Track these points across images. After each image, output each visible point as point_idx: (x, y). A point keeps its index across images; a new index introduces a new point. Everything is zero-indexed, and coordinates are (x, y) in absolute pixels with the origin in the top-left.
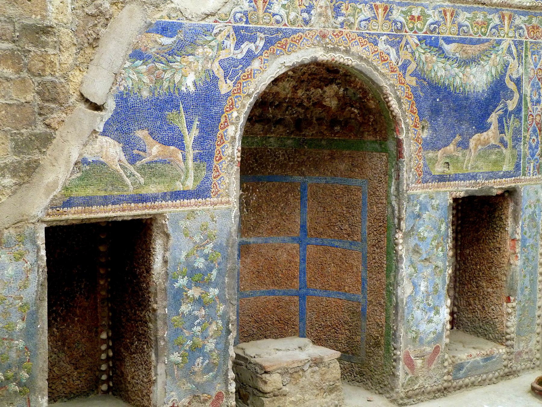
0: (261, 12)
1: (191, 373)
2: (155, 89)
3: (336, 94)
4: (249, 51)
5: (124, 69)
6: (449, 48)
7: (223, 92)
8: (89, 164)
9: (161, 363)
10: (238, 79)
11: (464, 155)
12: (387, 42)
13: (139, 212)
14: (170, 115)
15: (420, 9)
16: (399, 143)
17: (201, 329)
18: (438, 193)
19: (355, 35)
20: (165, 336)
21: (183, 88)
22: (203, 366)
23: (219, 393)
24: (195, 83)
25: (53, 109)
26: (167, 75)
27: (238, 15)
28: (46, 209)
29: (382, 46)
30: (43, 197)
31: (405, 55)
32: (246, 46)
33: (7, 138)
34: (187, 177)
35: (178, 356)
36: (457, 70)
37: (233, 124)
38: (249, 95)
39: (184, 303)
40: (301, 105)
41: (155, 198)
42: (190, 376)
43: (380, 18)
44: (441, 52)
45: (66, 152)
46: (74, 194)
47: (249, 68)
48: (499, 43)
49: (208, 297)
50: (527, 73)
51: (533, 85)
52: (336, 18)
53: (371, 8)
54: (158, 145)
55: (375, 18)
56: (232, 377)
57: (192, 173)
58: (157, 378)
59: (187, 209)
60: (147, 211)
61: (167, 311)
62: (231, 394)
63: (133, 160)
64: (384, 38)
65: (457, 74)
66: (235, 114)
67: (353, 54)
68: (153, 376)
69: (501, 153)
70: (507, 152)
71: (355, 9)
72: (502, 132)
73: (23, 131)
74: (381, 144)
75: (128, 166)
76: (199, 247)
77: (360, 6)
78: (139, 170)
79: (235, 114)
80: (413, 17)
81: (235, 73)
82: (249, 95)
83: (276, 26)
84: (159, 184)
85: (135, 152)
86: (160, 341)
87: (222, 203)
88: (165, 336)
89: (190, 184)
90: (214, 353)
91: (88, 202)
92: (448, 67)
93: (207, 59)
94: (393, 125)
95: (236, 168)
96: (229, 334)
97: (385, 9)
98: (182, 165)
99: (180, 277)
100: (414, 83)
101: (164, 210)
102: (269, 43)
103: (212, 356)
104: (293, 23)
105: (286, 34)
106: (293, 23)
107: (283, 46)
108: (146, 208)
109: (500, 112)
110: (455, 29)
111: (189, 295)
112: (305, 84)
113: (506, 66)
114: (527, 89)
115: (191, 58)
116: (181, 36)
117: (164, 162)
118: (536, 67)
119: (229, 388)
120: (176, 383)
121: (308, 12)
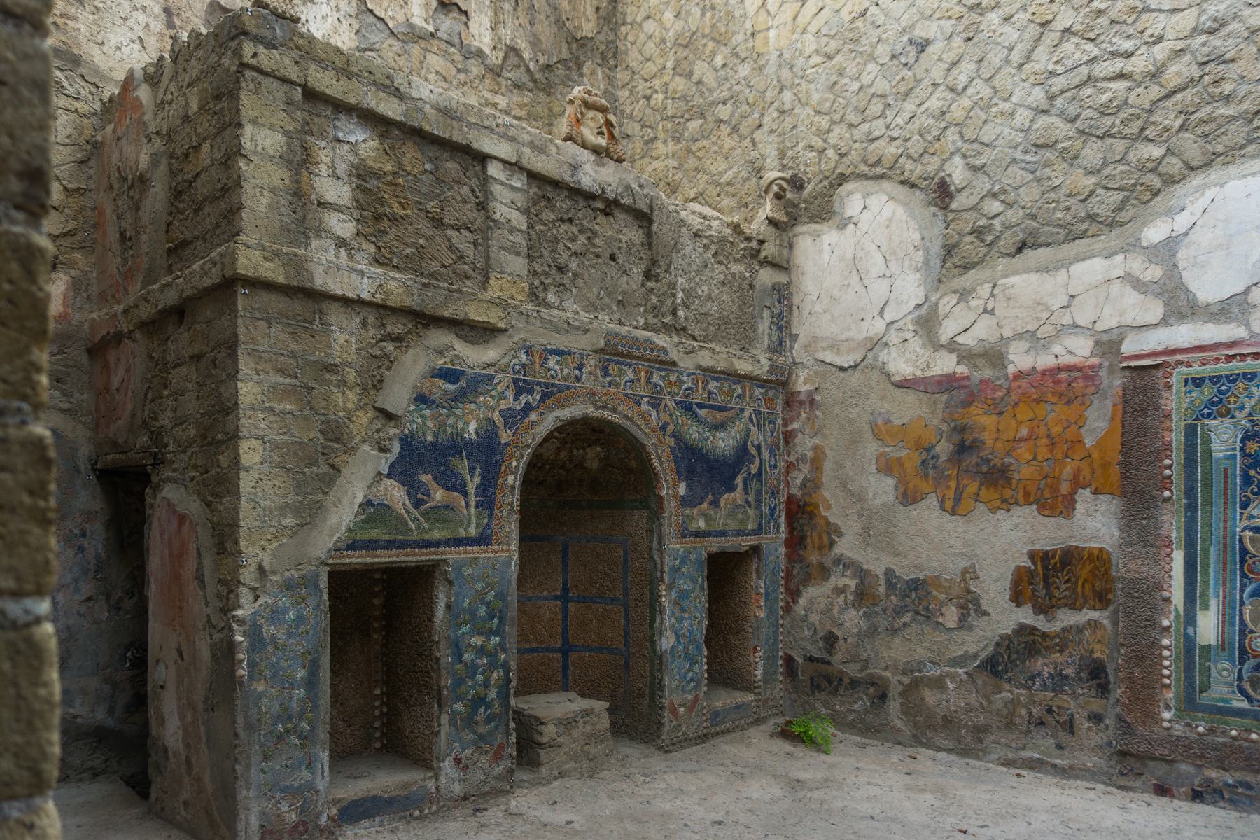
0: (537, 366)
2: (439, 433)
3: (598, 454)
4: (527, 403)
5: (409, 412)
6: (700, 412)
7: (503, 442)
8: (373, 506)
10: (517, 429)
11: (716, 513)
12: (648, 403)
13: (423, 558)
14: (454, 461)
15: (676, 374)
16: (660, 499)
18: (695, 548)
19: (620, 395)
21: (466, 436)
24: (476, 431)
25: (337, 449)
26: (450, 421)
27: (517, 367)
28: (329, 551)
29: (644, 407)
30: (327, 538)
31: (665, 417)
32: (524, 398)
33: (288, 476)
34: (469, 524)
36: (708, 434)
37: (512, 473)
38: (528, 446)
40: (563, 467)
41: (438, 544)
43: (643, 380)
44: (695, 415)
45: (350, 493)
46: (358, 537)
47: (527, 419)
48: (742, 411)
50: (765, 440)
51: (770, 452)
52: (605, 377)
53: (635, 370)
54: (441, 491)
55: (638, 380)
57: (474, 521)
59: (469, 556)
60: (430, 557)
63: (417, 504)
64: (646, 399)
65: (708, 438)
66: (514, 464)
67: (620, 413)
69: (746, 512)
70: (751, 512)
71: (621, 370)
72: (747, 494)
73: (306, 470)
74: (641, 502)
75: (413, 510)
76: (481, 596)
77: (626, 368)
78: (422, 515)
79: (514, 464)
80: (670, 383)
81: (515, 423)
82: (528, 446)
83: (551, 381)
84: (443, 529)
85: (420, 496)
87: (503, 551)
89: (473, 531)
91: (371, 545)
92: (701, 430)
93: (489, 408)
94: (655, 483)
95: (516, 517)
97: (647, 373)
98: (465, 511)
100: (672, 444)
101: (447, 556)
102: (545, 396)
104: (566, 380)
105: (561, 389)
106: (566, 380)
107: (558, 401)
108: (430, 553)
109: (745, 475)
110: (706, 396)
112: (568, 446)
113: (748, 433)
114: (766, 454)
115: (473, 406)
116: (463, 383)
117: (447, 507)
118: (772, 435)
121: (580, 371)
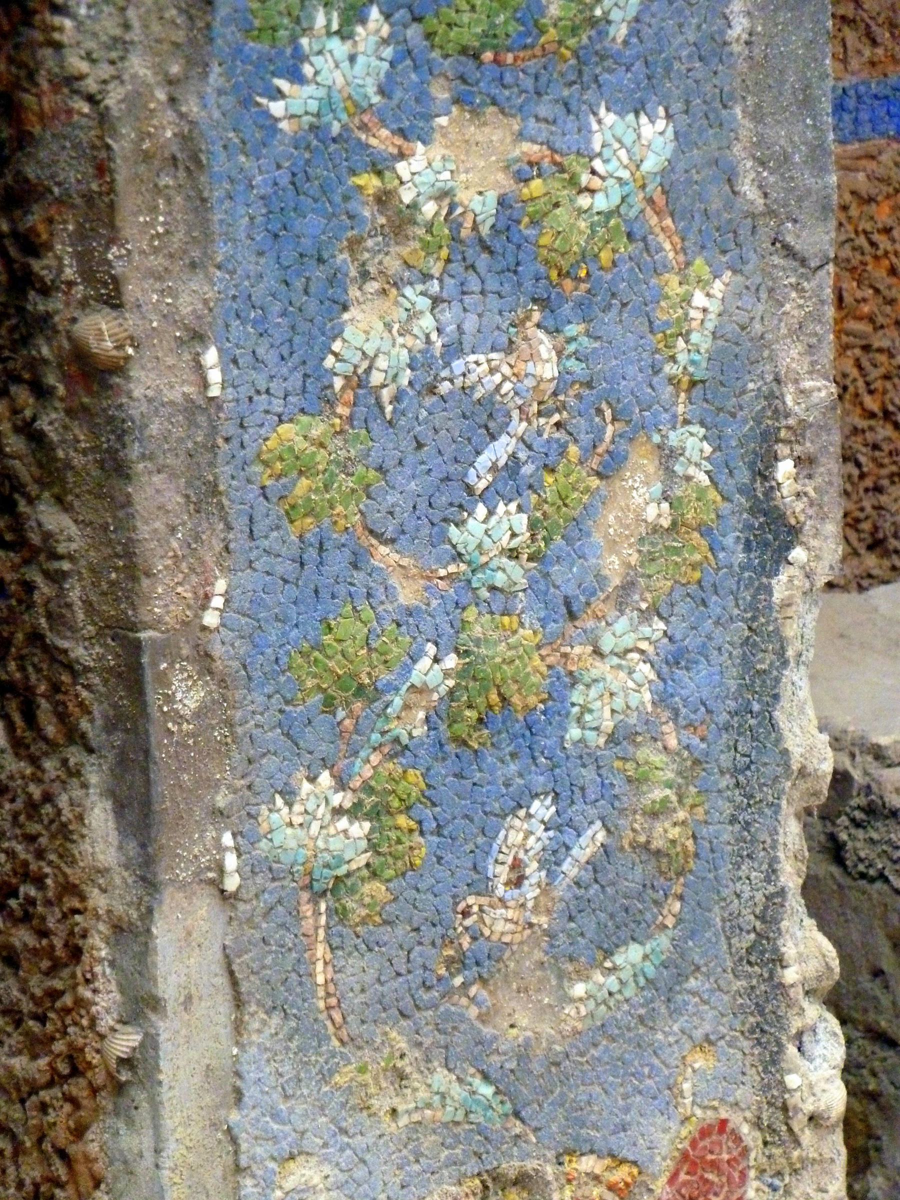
1: (458, 963)
9: (183, 886)
17: (533, 526)
20: (211, 619)
22: (561, 889)
23: (704, 1133)
35: (338, 812)
39: (365, 275)
42: (447, 994)
49: (584, 201)
56: (813, 967)
58: (150, 1043)
61: (215, 376)
62: (807, 1137)
68: (106, 1022)
86: (163, 680)
88: (211, 619)
90: (649, 754)
96: (780, 557)
99: (320, 20)
103: (637, 782)
111: (407, 196)
119: (792, 1081)
120: (325, 1077)
